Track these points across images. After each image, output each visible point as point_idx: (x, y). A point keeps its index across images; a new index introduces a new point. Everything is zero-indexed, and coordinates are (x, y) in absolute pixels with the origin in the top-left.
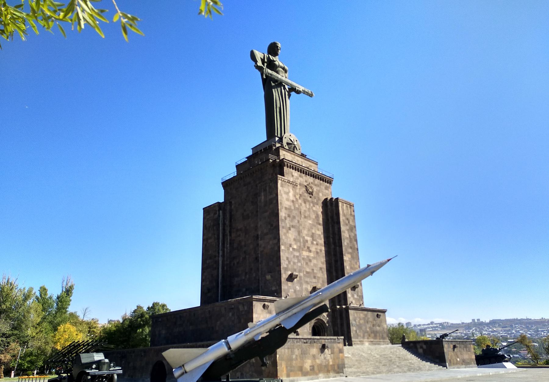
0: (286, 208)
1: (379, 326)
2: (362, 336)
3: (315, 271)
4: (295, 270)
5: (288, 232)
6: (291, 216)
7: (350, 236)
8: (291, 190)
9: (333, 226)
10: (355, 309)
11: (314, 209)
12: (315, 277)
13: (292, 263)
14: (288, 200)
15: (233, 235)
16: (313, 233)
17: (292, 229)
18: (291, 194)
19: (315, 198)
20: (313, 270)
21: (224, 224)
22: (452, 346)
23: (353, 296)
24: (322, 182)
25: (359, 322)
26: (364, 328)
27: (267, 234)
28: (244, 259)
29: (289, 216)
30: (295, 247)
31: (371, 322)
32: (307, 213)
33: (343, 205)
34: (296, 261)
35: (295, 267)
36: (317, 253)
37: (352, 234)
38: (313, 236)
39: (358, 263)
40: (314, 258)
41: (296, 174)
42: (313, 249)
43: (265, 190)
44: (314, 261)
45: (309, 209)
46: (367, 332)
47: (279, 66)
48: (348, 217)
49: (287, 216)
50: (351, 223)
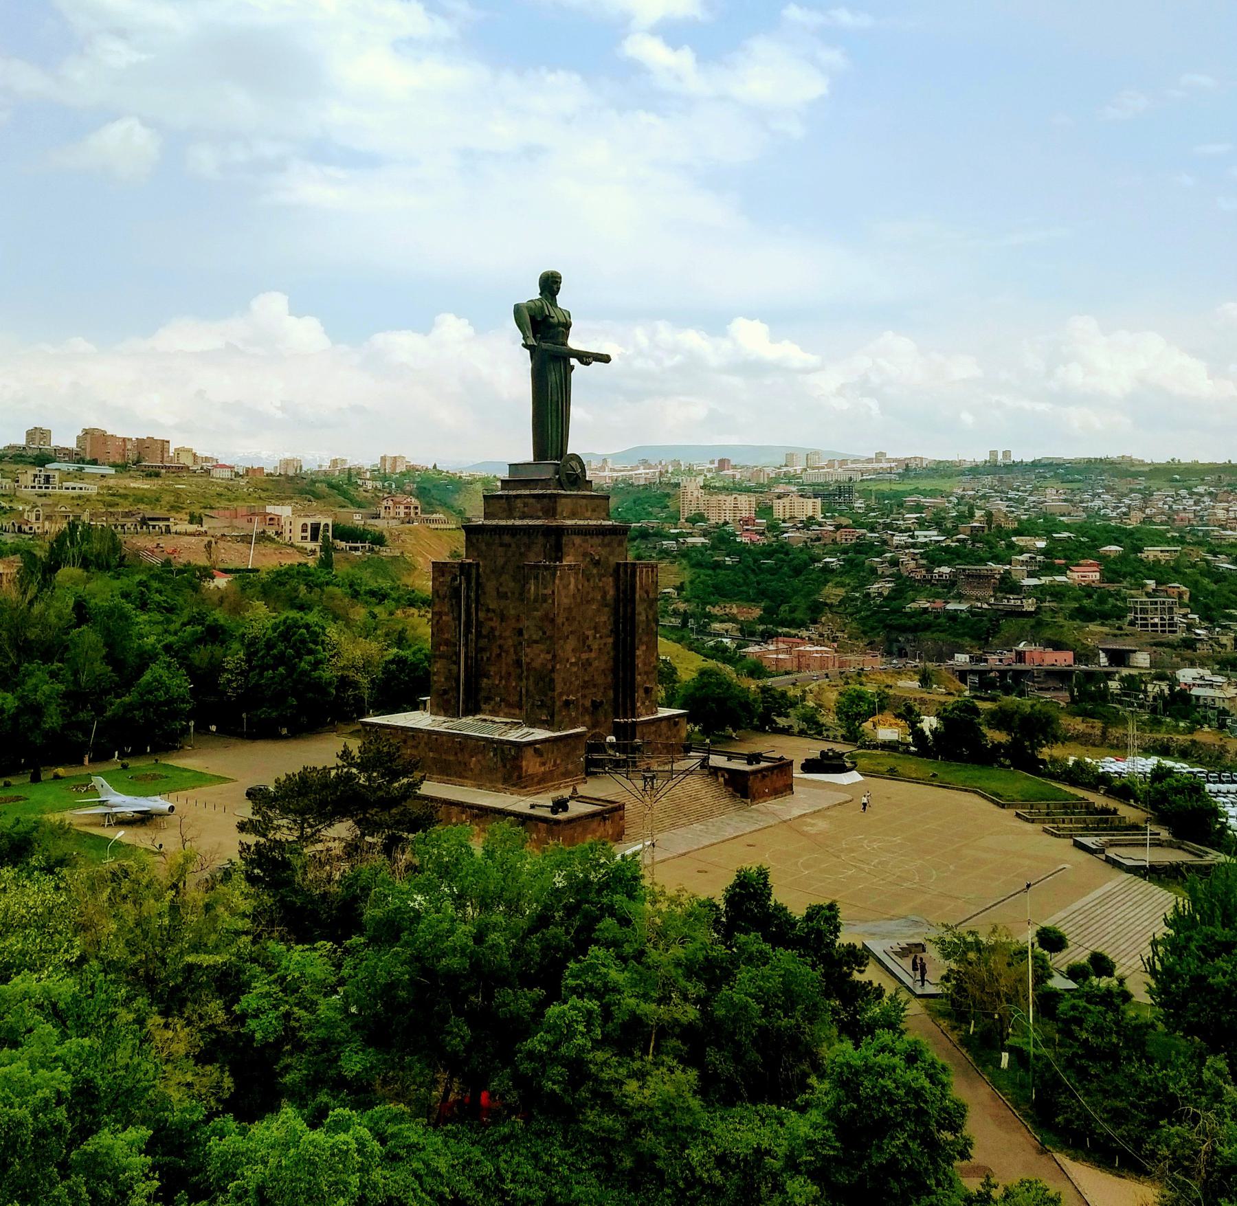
8: (572, 580)
9: (625, 606)
12: (595, 686)
15: (482, 615)
18: (572, 586)
21: (468, 597)
23: (643, 703)
27: (536, 642)
28: (499, 655)
33: (641, 572)
41: (578, 540)
42: (595, 646)
43: (536, 578)
44: (596, 663)
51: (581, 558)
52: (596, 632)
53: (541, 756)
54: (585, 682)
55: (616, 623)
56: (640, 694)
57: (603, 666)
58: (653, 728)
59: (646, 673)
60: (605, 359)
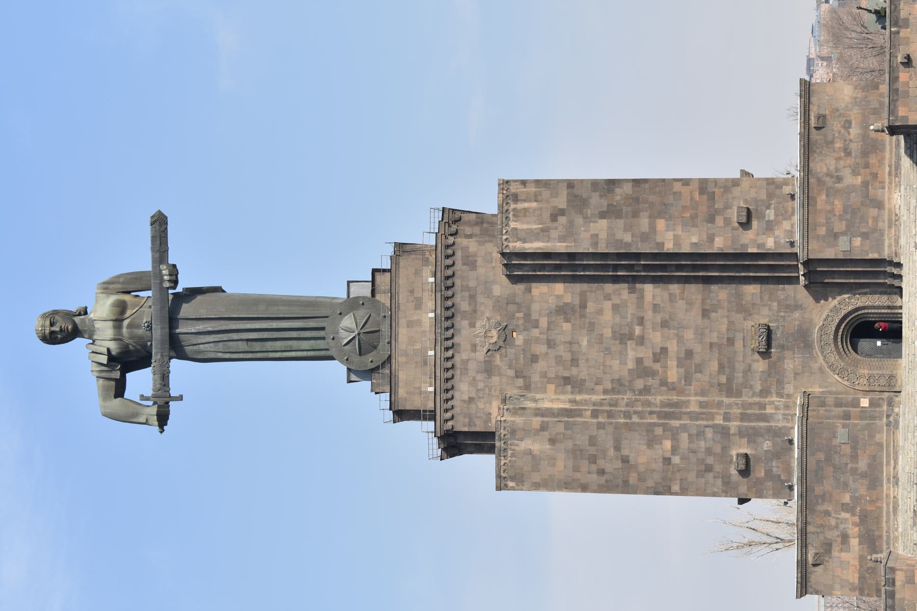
0: (576, 469)
1: (848, 125)
2: (873, 212)
3: (715, 340)
4: (725, 449)
5: (635, 467)
6: (592, 450)
7: (603, 215)
10: (807, 227)
11: (544, 322)
12: (731, 341)
13: (710, 460)
14: (552, 460)
16: (614, 338)
17: (625, 452)
19: (512, 317)
20: (711, 345)
22: (904, 75)
23: (770, 227)
24: (458, 282)
25: (841, 218)
26: (855, 199)
29: (593, 460)
30: (668, 444)
31: (838, 159)
32: (562, 350)
34: (702, 444)
35: (718, 449)
36: (665, 324)
38: (623, 337)
39: (677, 187)
40: (680, 339)
41: (463, 390)
42: (656, 338)
45: (550, 344)
46: (865, 184)
48: (546, 215)
49: (594, 467)
50: (561, 202)
51: (495, 379)
52: (631, 336)
53: (828, 547)
54: (721, 367)
55: (616, 280)
57: (694, 316)
58: (821, 200)
59: (711, 219)
60: (160, 223)
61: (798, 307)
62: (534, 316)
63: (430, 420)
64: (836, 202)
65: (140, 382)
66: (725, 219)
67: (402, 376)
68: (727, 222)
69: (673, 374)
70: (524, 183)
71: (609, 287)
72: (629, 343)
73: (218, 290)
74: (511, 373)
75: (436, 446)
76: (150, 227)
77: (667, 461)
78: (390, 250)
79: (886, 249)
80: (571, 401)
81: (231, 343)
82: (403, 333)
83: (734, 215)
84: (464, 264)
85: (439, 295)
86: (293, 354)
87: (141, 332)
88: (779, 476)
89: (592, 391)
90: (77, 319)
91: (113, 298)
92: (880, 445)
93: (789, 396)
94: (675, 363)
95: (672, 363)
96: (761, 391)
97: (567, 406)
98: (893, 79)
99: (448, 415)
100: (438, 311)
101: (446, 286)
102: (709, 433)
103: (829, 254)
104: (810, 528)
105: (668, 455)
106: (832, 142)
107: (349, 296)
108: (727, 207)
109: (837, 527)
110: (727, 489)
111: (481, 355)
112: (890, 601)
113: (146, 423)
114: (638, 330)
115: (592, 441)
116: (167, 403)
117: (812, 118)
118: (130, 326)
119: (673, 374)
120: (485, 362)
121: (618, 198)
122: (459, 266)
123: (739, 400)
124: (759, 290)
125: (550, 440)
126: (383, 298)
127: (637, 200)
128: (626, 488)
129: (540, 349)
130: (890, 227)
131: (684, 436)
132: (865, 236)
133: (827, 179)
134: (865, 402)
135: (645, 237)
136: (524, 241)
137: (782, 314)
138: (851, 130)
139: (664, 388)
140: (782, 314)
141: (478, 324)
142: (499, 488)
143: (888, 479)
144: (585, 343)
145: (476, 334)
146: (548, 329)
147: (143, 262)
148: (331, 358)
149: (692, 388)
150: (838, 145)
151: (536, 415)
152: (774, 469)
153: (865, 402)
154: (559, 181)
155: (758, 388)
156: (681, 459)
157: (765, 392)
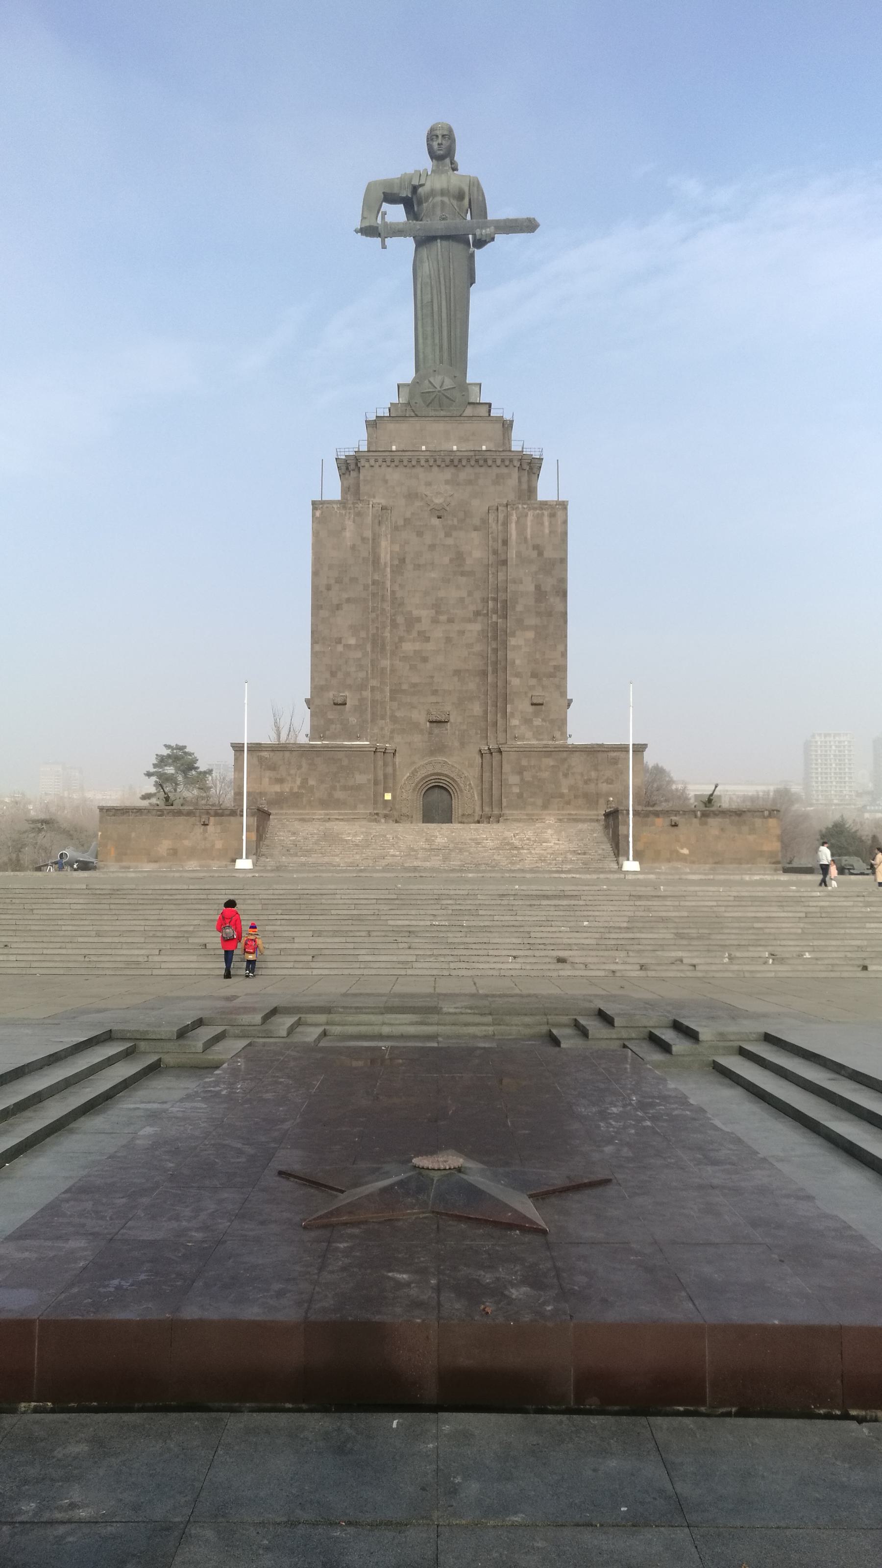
0: (331, 567)
1: (609, 781)
2: (539, 802)
4: (350, 687)
7: (538, 587)
10: (527, 752)
11: (450, 541)
12: (435, 692)
13: (340, 675)
20: (432, 677)
23: (527, 721)
24: (482, 470)
29: (339, 581)
30: (352, 641)
31: (582, 775)
34: (353, 669)
36: (448, 640)
37: (549, 583)
38: (437, 607)
39: (560, 648)
41: (395, 476)
45: (432, 547)
46: (562, 796)
47: (432, 193)
49: (332, 581)
50: (549, 553)
53: (273, 768)
54: (414, 685)
56: (521, 706)
58: (550, 762)
59: (534, 675)
61: (463, 745)
62: (454, 534)
63: (368, 448)
64: (547, 773)
65: (396, 214)
66: (534, 686)
67: (404, 426)
68: (532, 688)
69: (408, 647)
70: (565, 522)
71: (478, 595)
72: (434, 611)
73: (472, 281)
74: (408, 515)
75: (347, 454)
76: (525, 217)
77: (339, 641)
78: (508, 417)
79: (511, 812)
80: (385, 564)
81: (429, 288)
82: (440, 427)
83: (538, 692)
84: (497, 475)
85: (472, 454)
86: (421, 341)
87: (438, 212)
88: (328, 730)
89: (393, 581)
90: (448, 161)
91: (466, 189)
92: (355, 807)
93: (392, 738)
94: (417, 648)
95: (417, 646)
96: (396, 717)
97: (382, 561)
98: (657, 814)
99: (372, 462)
100: (458, 454)
101: (479, 460)
102: (362, 675)
103: (506, 768)
104: (287, 754)
105: (344, 642)
106: (596, 770)
107: (469, 384)
108: (543, 687)
109: (289, 775)
110: (317, 689)
111: (423, 489)
112: (227, 812)
113: (363, 218)
114: (443, 618)
115: (354, 580)
116: (379, 235)
117: (615, 754)
118: (443, 202)
119: (408, 647)
120: (417, 494)
121: (552, 600)
122: (495, 471)
123: (388, 699)
124: (476, 714)
125: (354, 545)
126: (469, 411)
127: (550, 614)
128: (316, 608)
129: (428, 539)
130: (527, 815)
131: (359, 655)
132: (520, 796)
133: (566, 766)
134: (388, 796)
135: (520, 621)
136: (517, 522)
137: (457, 733)
138: (605, 784)
139: (397, 640)
140: (457, 733)
141: (448, 487)
142: (314, 503)
143: (327, 814)
144: (433, 575)
145: (439, 487)
146: (444, 545)
147: (495, 213)
148: (417, 370)
149: (398, 662)
150: (593, 774)
151: (374, 534)
152: (334, 726)
153: (388, 796)
154: (566, 551)
155: (398, 714)
156: (341, 653)
157: (394, 719)
